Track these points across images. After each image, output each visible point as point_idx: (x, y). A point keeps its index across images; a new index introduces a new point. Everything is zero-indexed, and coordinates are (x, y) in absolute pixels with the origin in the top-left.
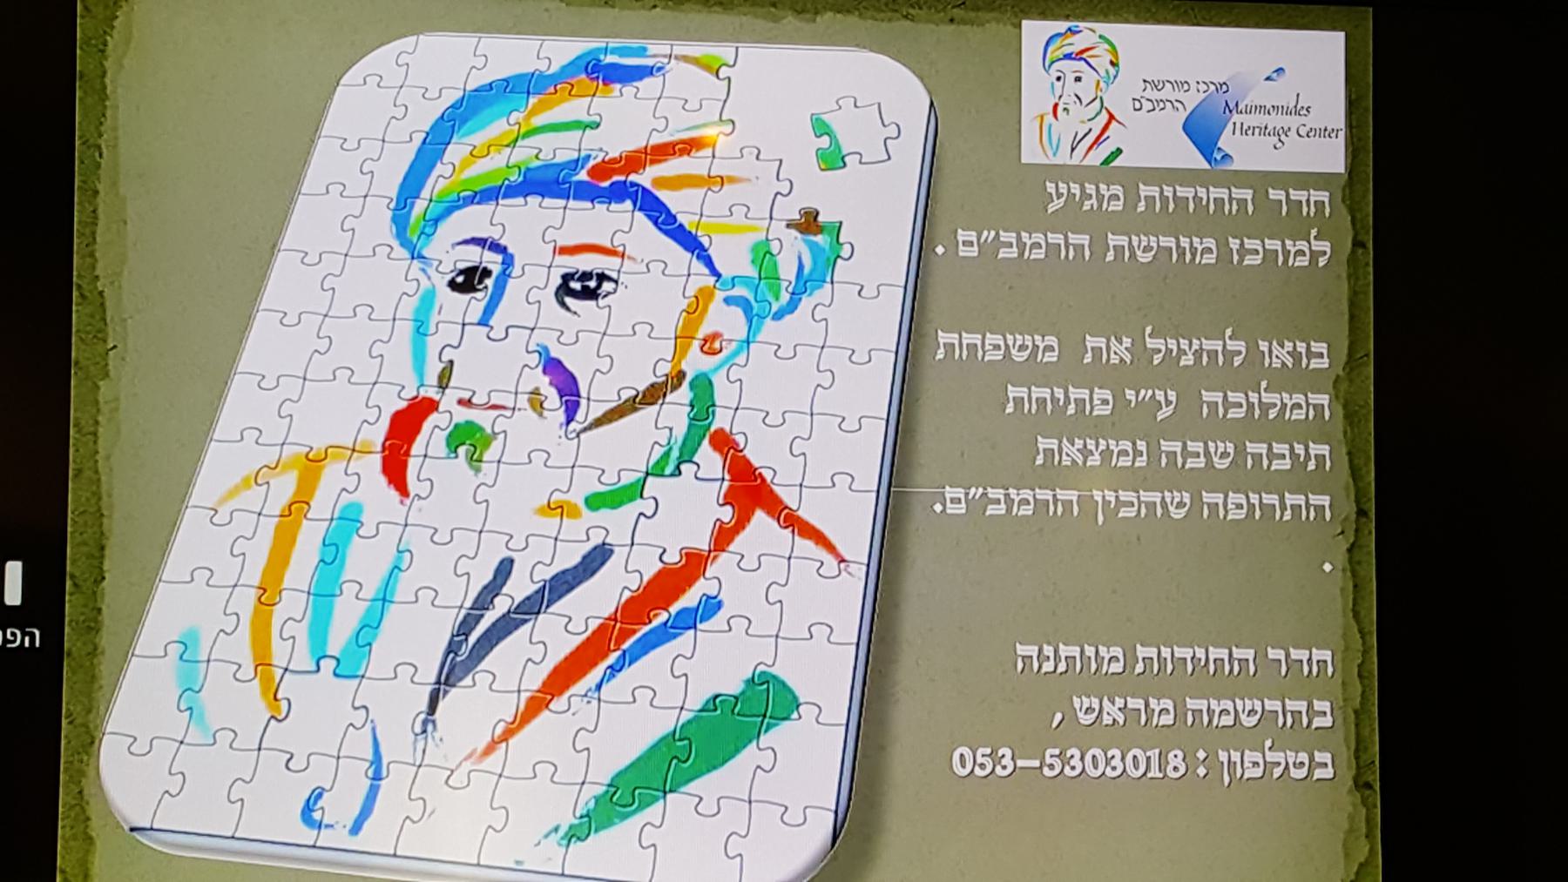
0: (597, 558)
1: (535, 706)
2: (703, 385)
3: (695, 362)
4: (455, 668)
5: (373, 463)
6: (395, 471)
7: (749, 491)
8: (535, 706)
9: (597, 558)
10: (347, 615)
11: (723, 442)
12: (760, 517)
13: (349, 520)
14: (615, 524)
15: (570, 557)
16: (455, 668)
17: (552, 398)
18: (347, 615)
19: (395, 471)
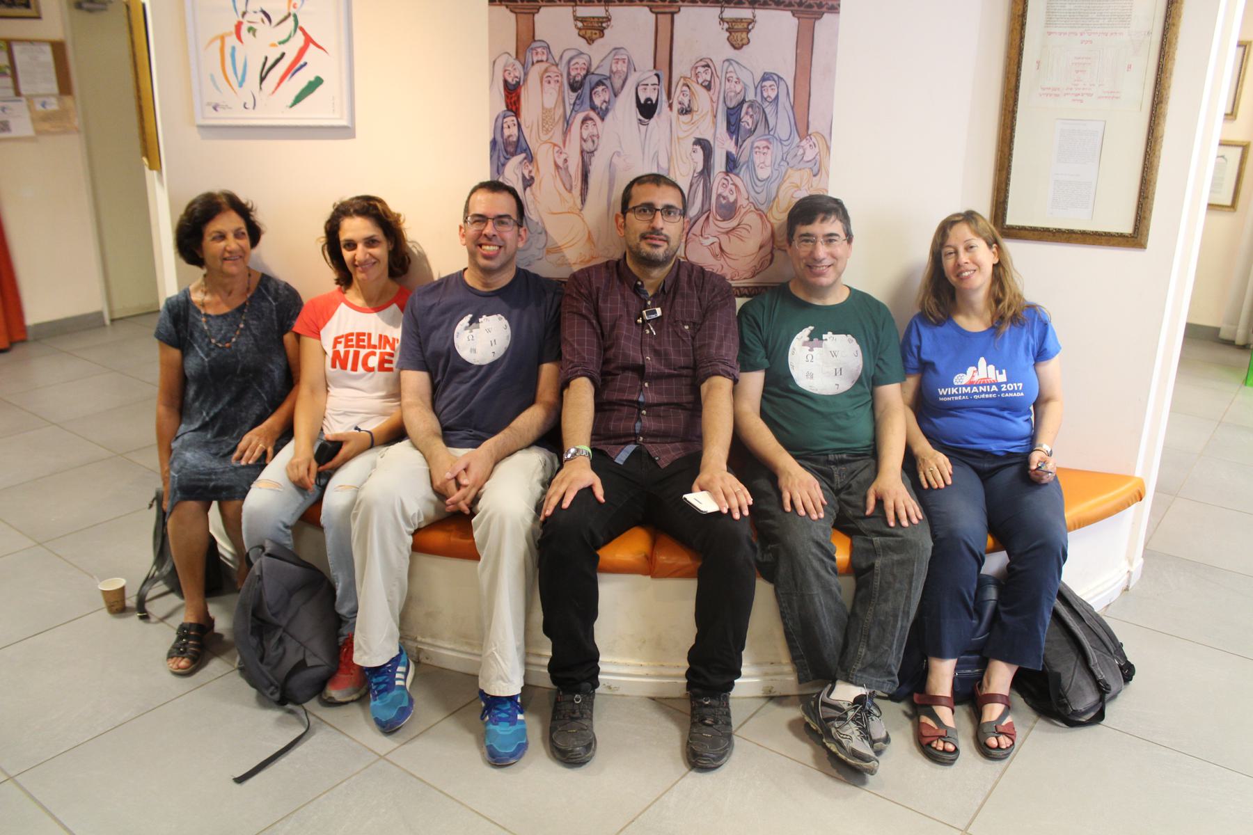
0: (283, 55)
1: (279, 85)
2: (295, 16)
3: (293, 11)
4: (262, 79)
5: (234, 36)
6: (239, 37)
7: (309, 40)
8: (279, 85)
9: (283, 55)
10: (240, 72)
11: (302, 29)
12: (312, 46)
13: (234, 48)
14: (282, 48)
15: (278, 56)
16: (262, 79)
17: (266, 20)
18: (240, 72)
19: (239, 37)
